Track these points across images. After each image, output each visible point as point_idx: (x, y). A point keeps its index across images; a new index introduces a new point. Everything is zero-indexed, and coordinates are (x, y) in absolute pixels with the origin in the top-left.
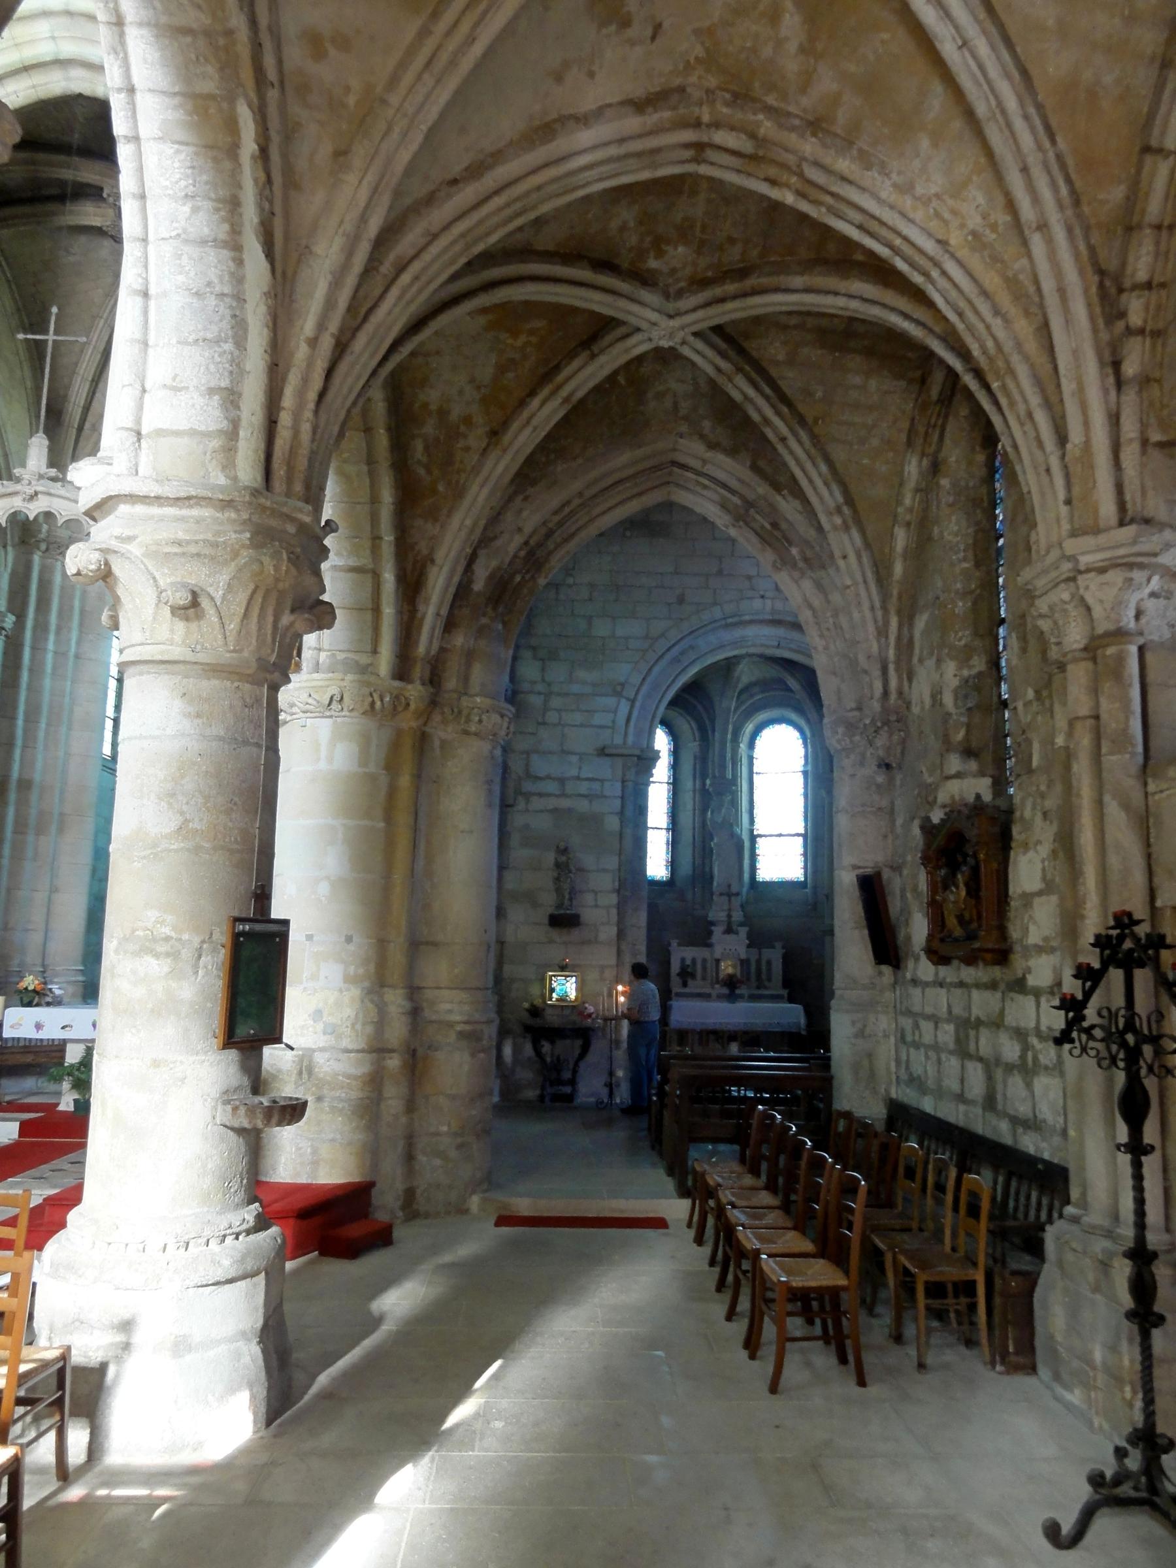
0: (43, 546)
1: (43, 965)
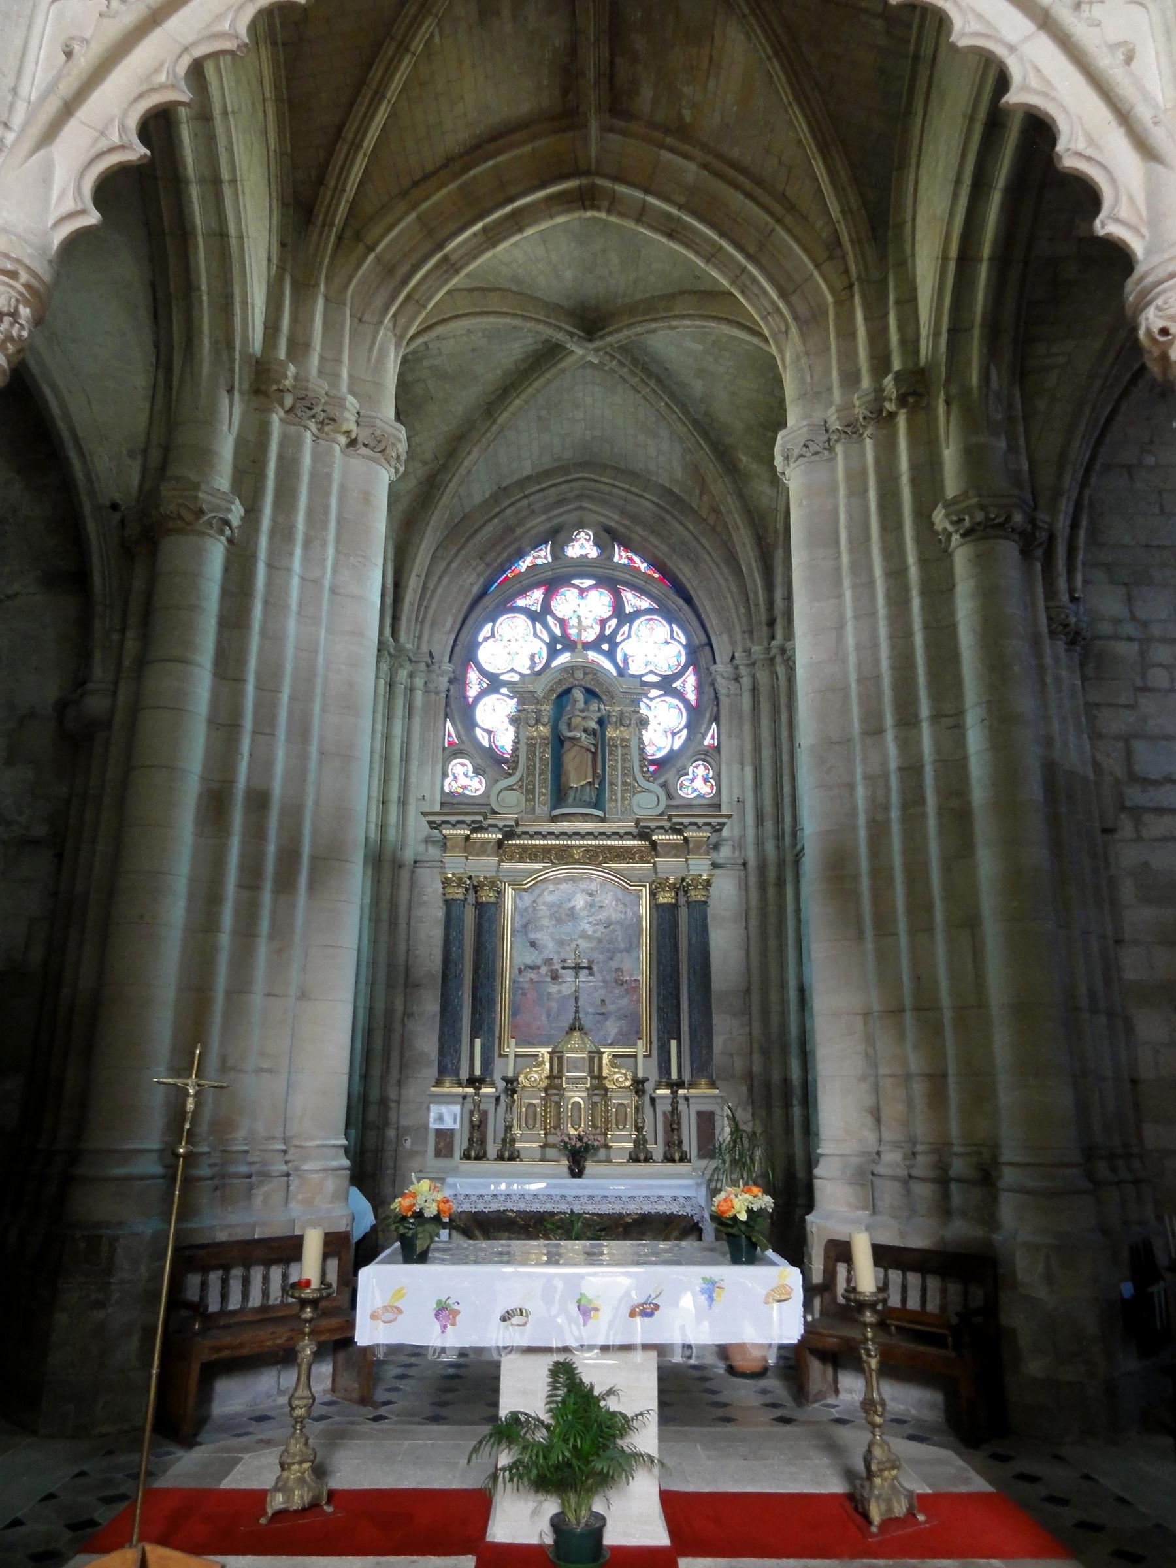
0: (289, 401)
1: (286, 1140)
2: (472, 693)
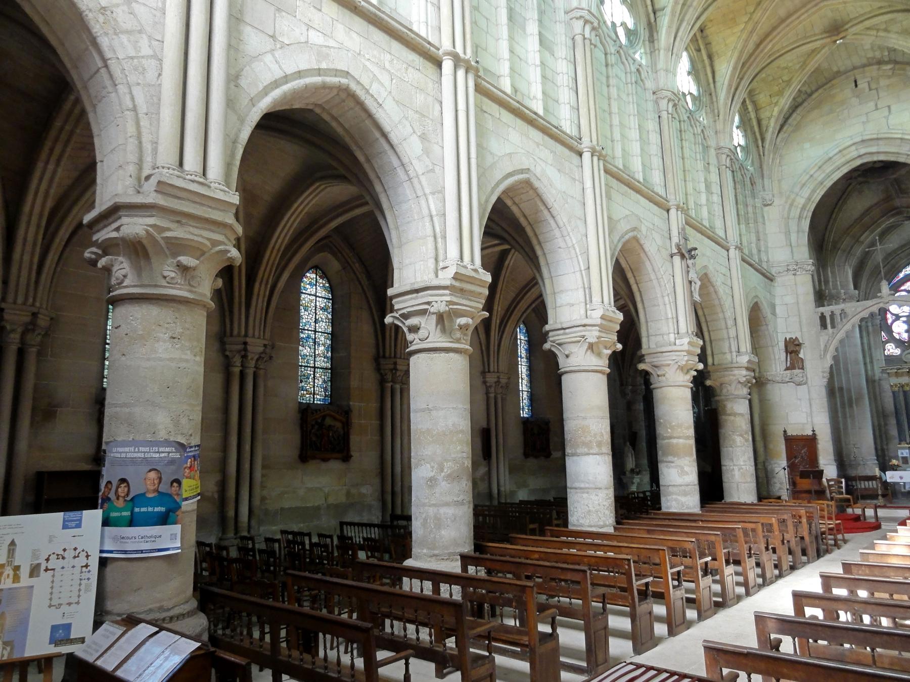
2: (890, 321)
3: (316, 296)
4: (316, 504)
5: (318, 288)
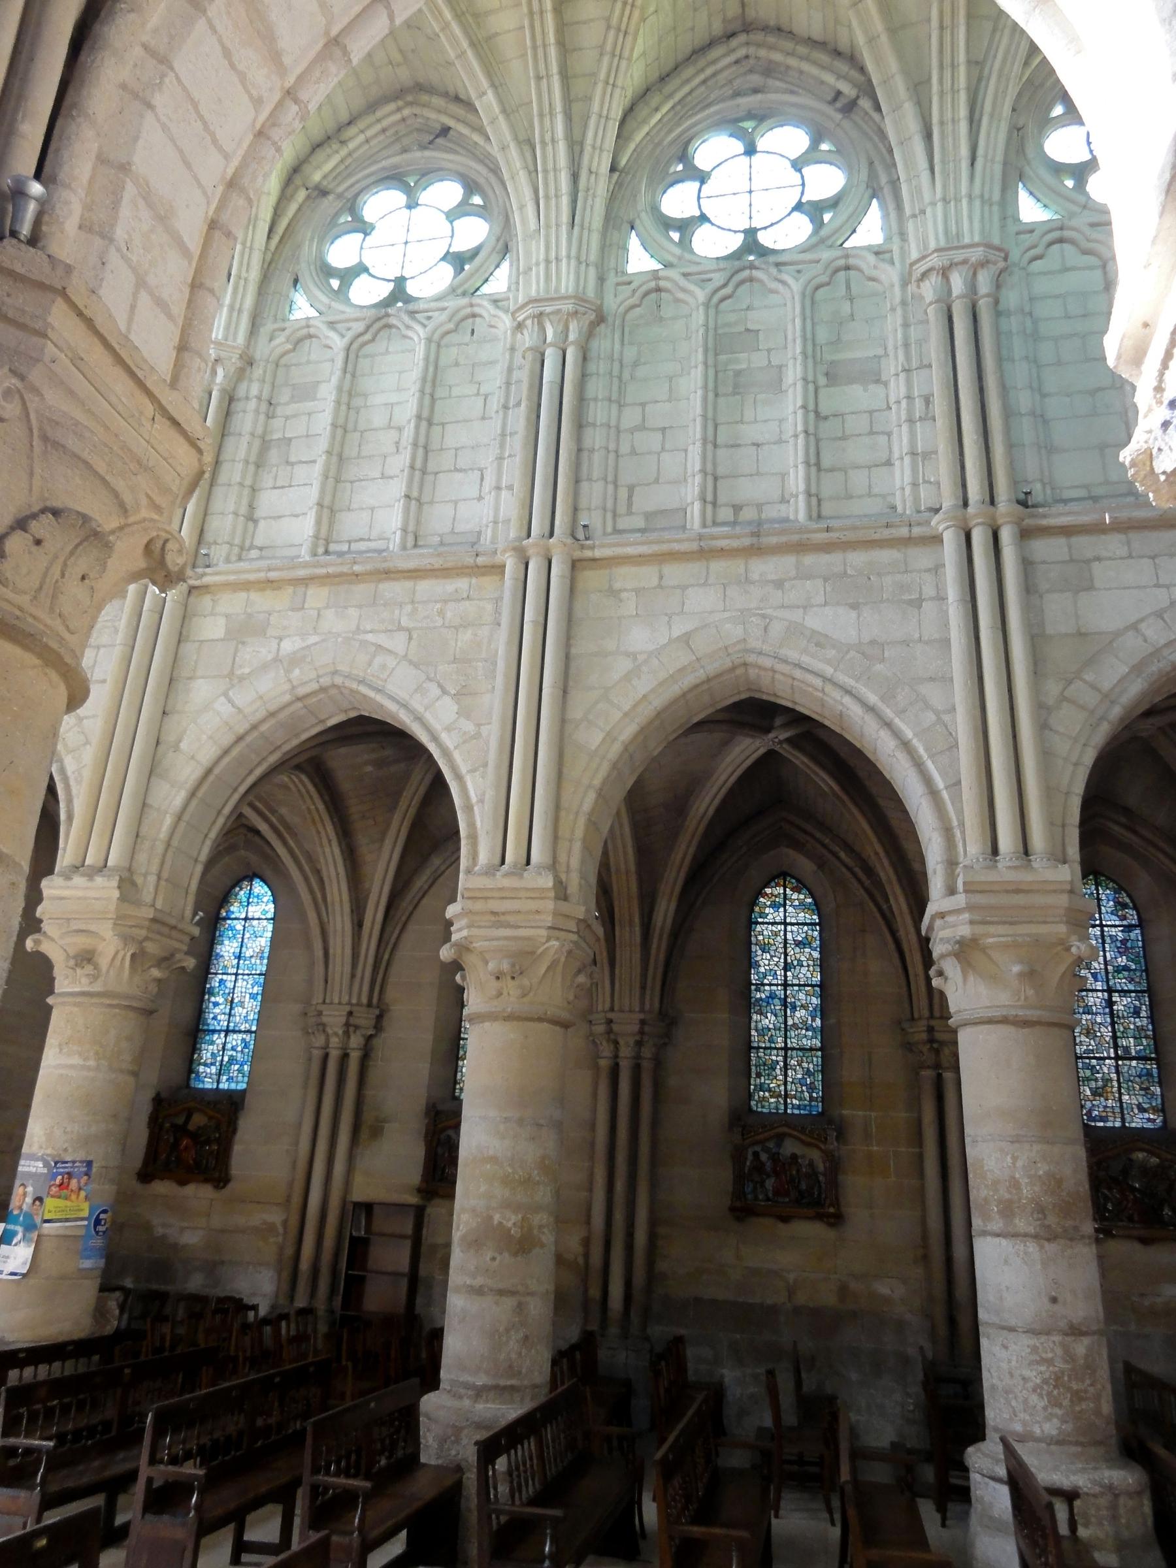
3: (785, 924)
4: (769, 1302)
5: (790, 909)
